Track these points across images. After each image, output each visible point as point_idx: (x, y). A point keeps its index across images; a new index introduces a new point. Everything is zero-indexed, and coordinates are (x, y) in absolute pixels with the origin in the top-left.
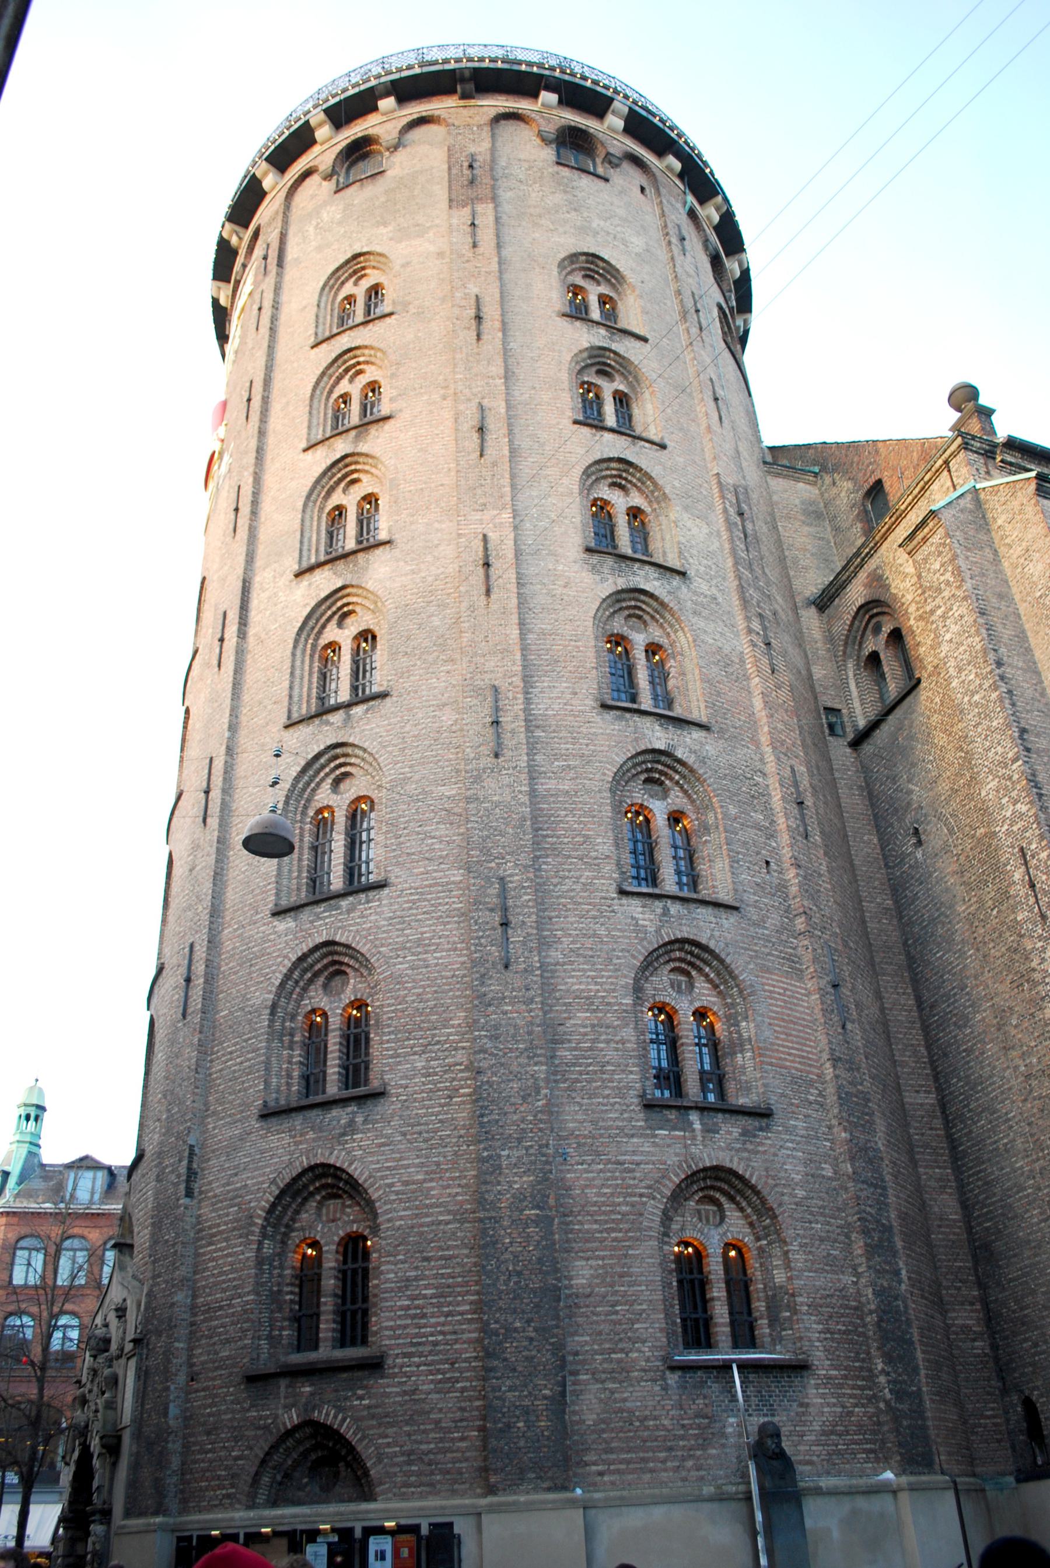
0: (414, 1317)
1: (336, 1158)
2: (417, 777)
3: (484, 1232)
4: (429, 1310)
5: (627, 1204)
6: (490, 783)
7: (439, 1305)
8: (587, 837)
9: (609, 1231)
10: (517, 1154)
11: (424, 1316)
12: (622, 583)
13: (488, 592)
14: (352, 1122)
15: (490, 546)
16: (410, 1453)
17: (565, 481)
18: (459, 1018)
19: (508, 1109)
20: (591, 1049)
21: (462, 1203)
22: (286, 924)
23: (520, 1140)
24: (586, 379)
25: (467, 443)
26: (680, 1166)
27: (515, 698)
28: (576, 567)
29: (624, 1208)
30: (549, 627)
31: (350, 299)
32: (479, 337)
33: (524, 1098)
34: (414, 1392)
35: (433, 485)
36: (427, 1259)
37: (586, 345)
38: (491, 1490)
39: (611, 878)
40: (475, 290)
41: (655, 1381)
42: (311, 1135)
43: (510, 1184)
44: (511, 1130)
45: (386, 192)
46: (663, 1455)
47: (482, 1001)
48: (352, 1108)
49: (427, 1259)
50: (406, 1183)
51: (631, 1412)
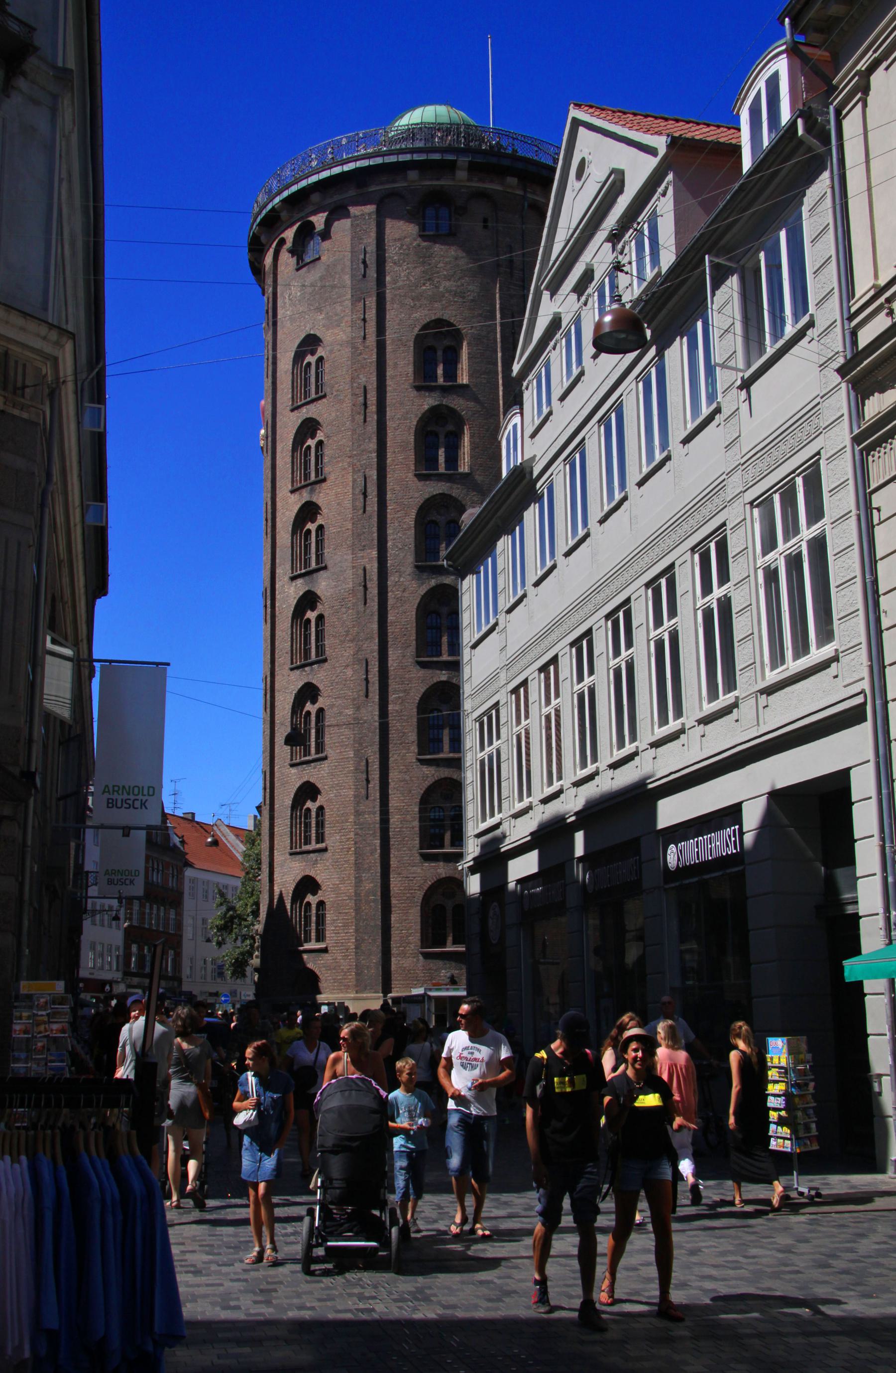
0: (336, 933)
1: (312, 874)
2: (337, 704)
3: (356, 904)
4: (340, 931)
5: (409, 893)
6: (363, 711)
7: (344, 930)
8: (404, 733)
9: (402, 903)
10: (367, 875)
11: (339, 933)
12: (433, 583)
13: (365, 603)
14: (316, 860)
15: (368, 575)
16: (334, 979)
17: (407, 520)
18: (352, 818)
19: (365, 858)
20: (399, 831)
21: (351, 893)
22: (294, 771)
23: (369, 870)
24: (429, 429)
25: (357, 504)
26: (433, 878)
27: (375, 665)
28: (409, 578)
29: (408, 895)
30: (394, 618)
31: (309, 364)
32: (365, 421)
33: (371, 854)
34: (336, 959)
35: (344, 529)
36: (340, 913)
37: (426, 407)
38: (357, 992)
39: (414, 752)
40: (363, 380)
41: (414, 957)
42: (304, 864)
43: (365, 887)
44: (366, 866)
45: (322, 278)
46: (415, 982)
47: (358, 813)
48: (316, 854)
49: (340, 913)
50: (333, 885)
51: (405, 968)
